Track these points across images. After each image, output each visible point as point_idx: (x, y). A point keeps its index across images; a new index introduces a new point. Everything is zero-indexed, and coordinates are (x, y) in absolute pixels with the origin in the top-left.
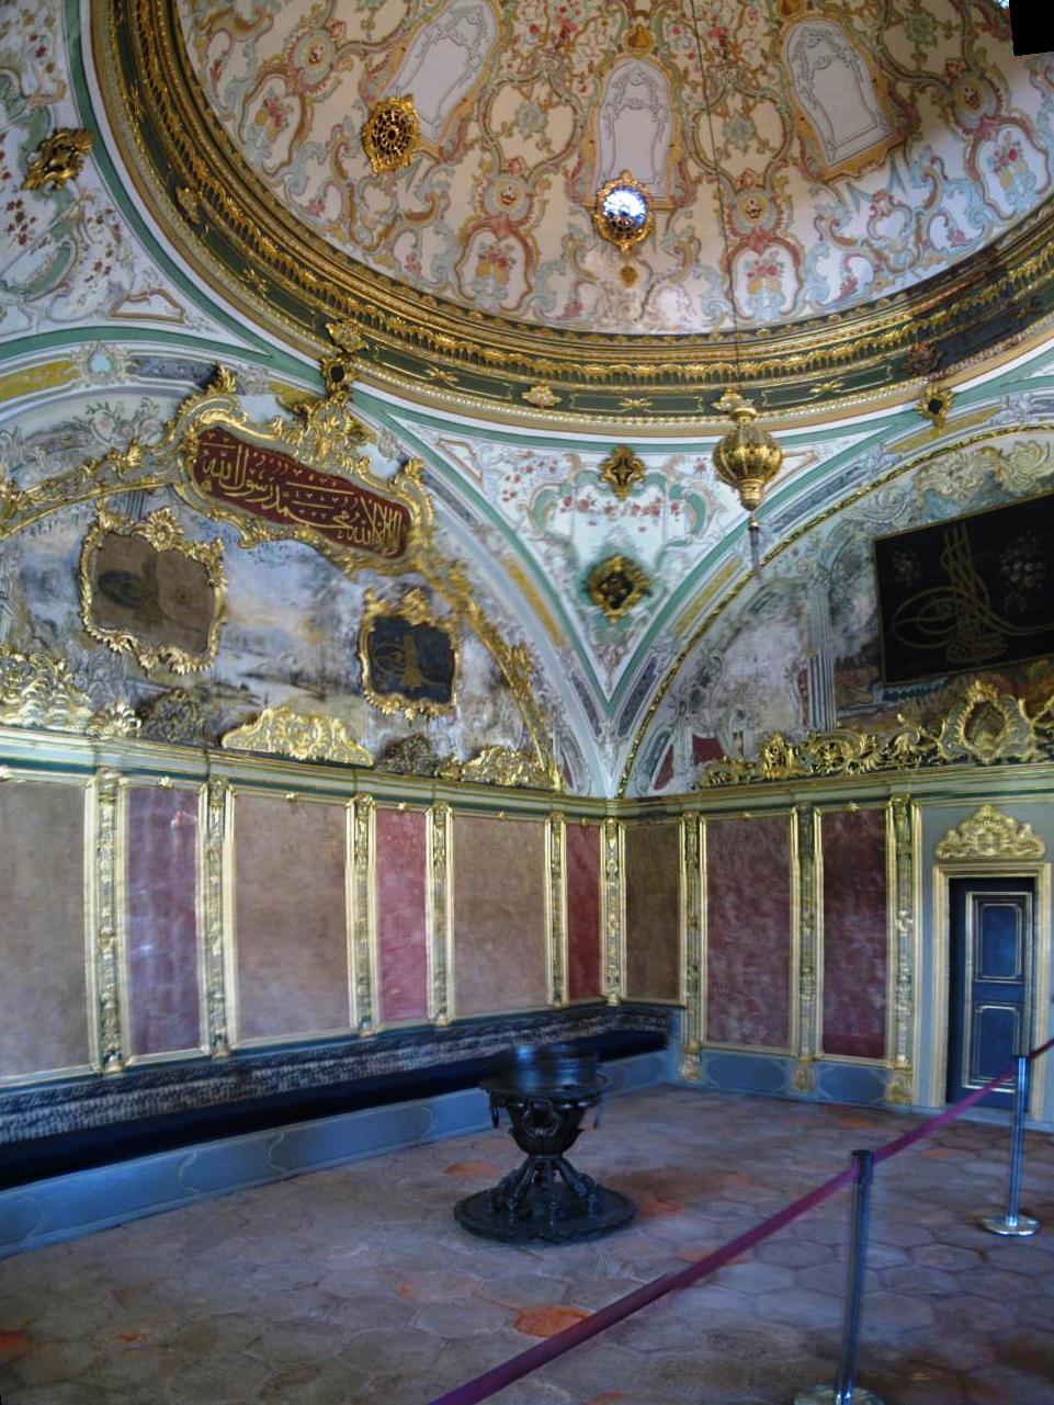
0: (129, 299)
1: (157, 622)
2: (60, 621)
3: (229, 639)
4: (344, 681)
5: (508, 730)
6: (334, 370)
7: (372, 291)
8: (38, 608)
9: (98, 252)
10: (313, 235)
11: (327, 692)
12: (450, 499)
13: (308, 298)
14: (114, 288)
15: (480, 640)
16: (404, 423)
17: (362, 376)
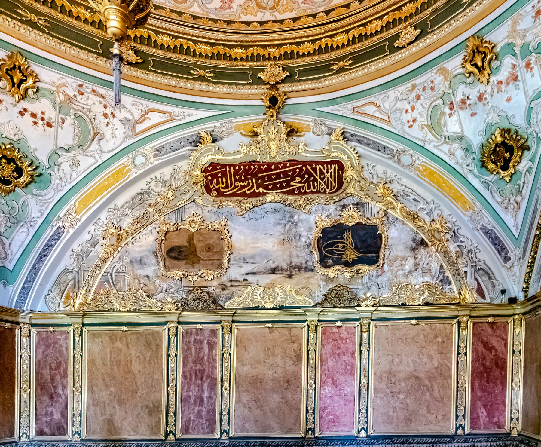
0: (137, 123)
1: (198, 262)
2: (151, 275)
3: (235, 260)
4: (304, 266)
5: (427, 271)
6: (270, 100)
7: (282, 36)
8: (141, 272)
9: (98, 109)
10: (229, 23)
11: (294, 273)
12: (369, 143)
13: (239, 65)
14: (124, 122)
15: (403, 223)
16: (328, 109)
17: (289, 95)
